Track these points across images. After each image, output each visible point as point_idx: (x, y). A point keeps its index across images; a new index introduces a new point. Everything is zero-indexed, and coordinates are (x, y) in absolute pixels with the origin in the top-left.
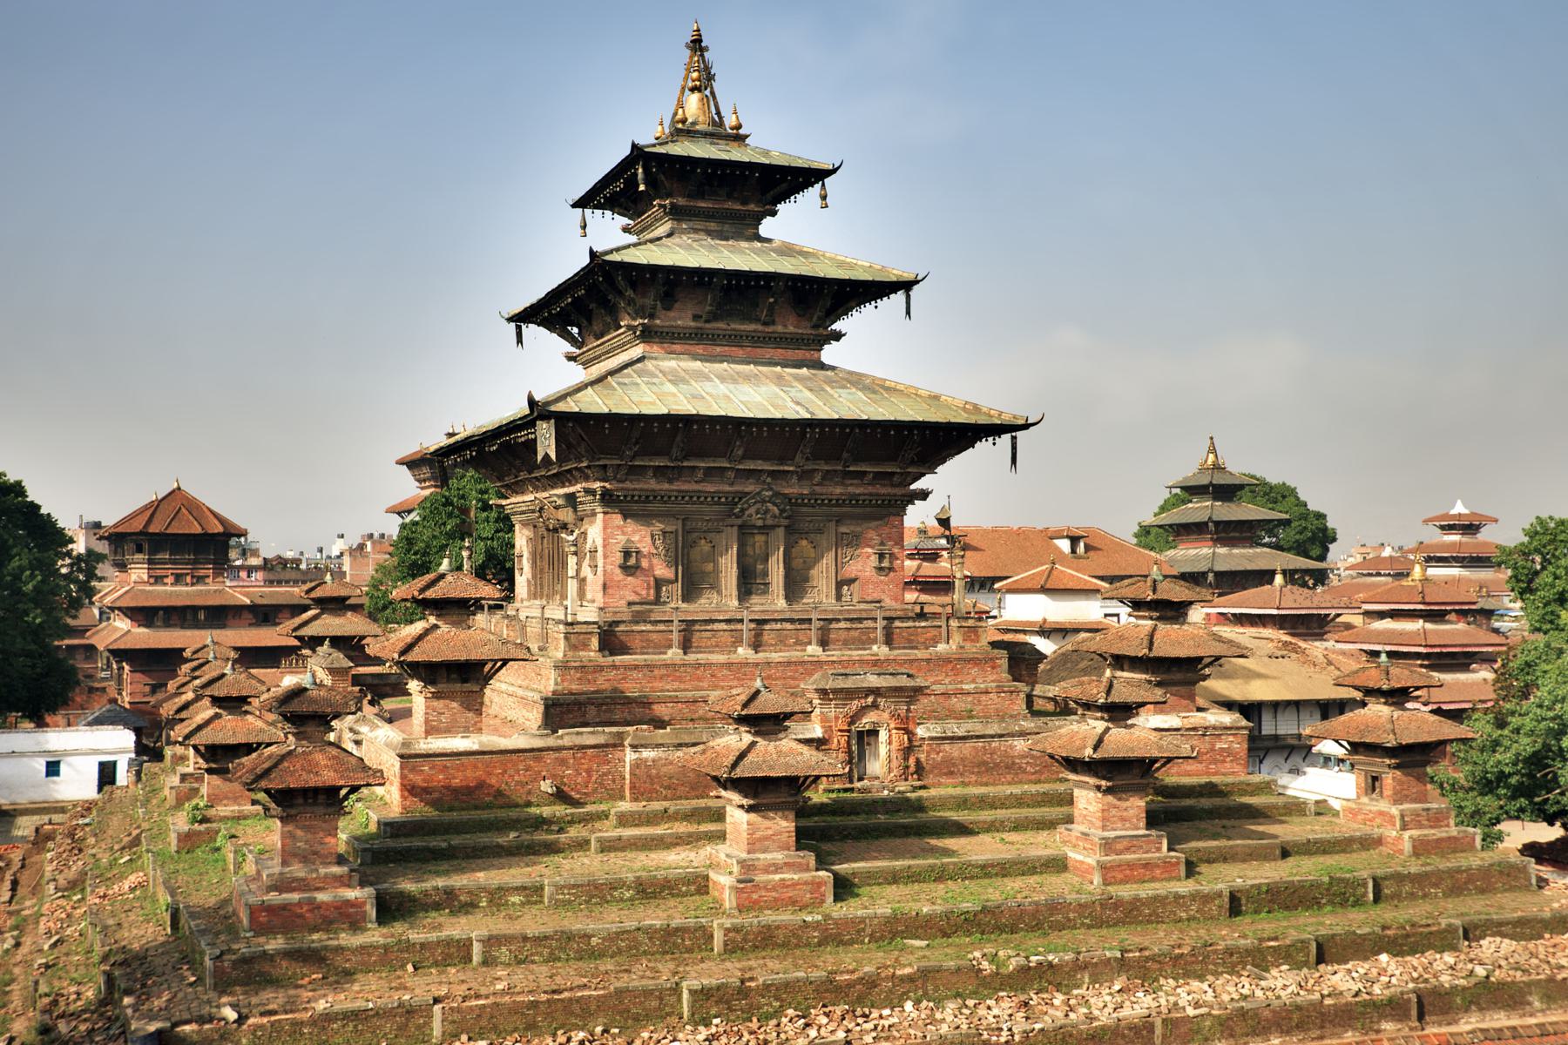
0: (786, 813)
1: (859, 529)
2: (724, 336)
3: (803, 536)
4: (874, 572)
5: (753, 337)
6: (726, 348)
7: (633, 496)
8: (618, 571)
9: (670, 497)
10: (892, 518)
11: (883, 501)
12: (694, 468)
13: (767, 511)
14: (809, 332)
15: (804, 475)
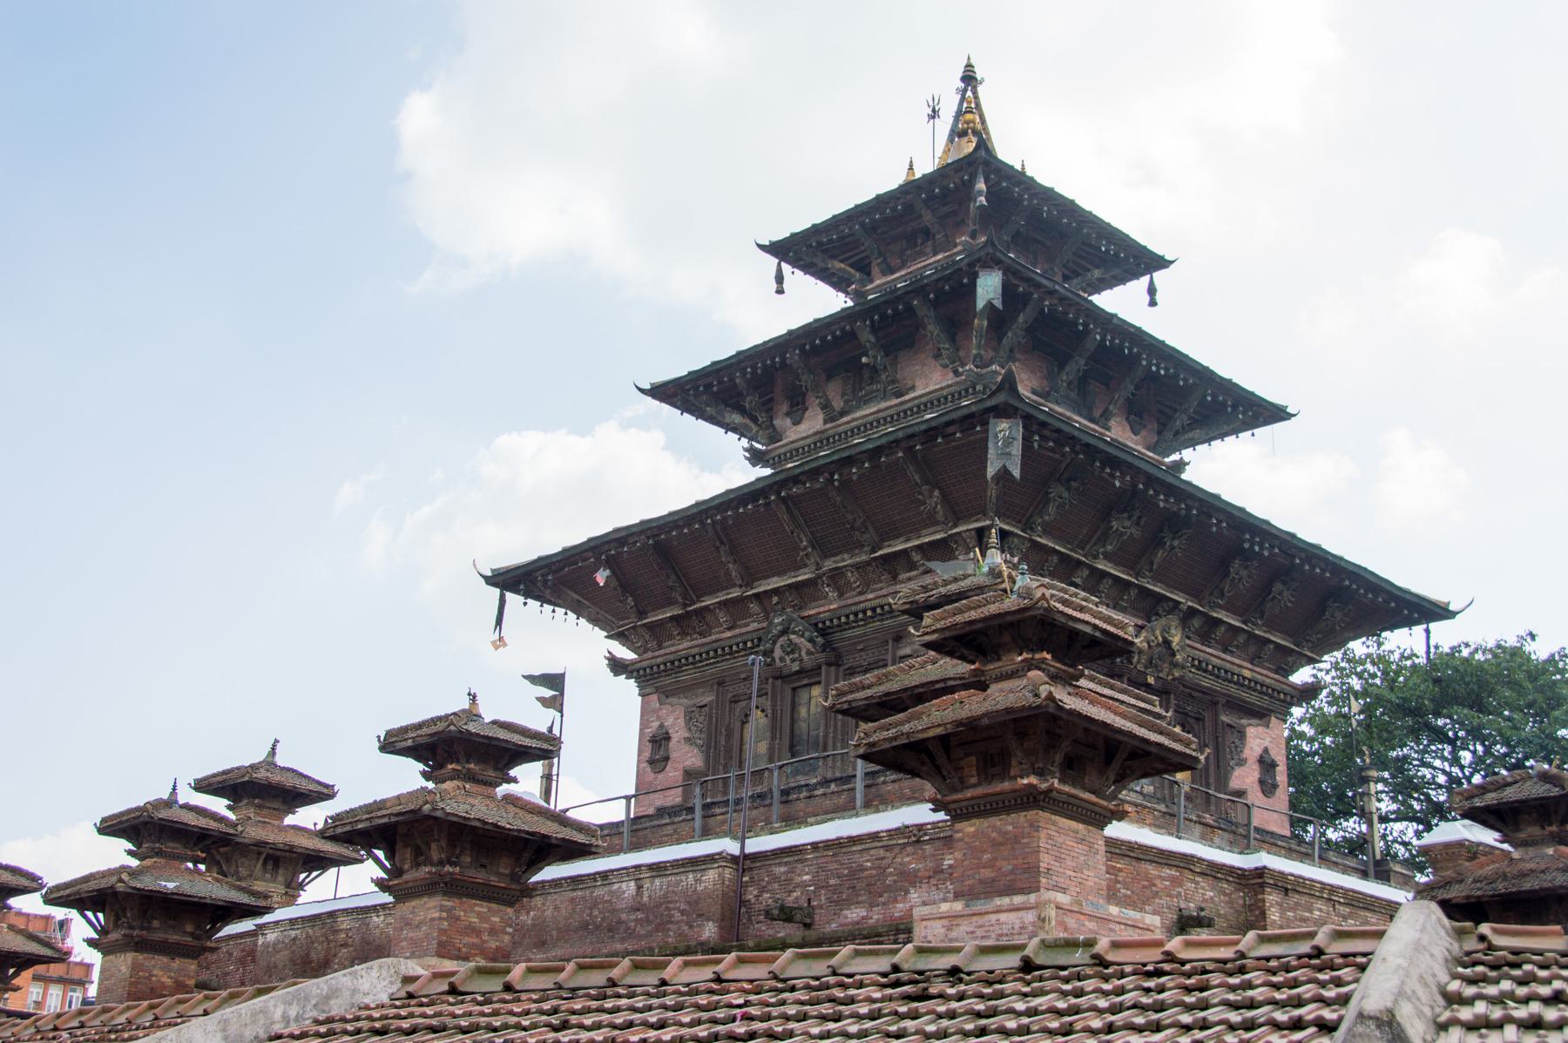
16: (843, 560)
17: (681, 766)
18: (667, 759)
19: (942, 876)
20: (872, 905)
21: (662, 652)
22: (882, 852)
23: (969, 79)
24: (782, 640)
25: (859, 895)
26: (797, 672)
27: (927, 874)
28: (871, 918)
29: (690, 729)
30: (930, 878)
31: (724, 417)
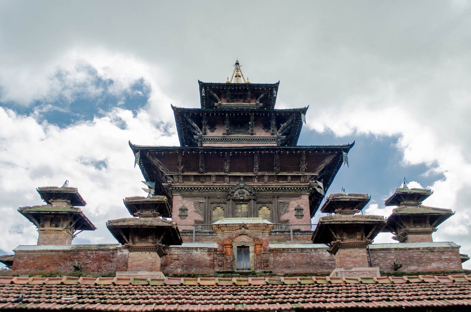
0: (151, 253)
1: (288, 200)
2: (235, 139)
3: (264, 205)
4: (295, 218)
5: (247, 139)
6: (237, 144)
7: (185, 188)
8: (179, 218)
9: (201, 188)
10: (303, 196)
11: (297, 188)
12: (210, 176)
13: (244, 193)
14: (269, 136)
15: (260, 178)
16: (265, 173)
17: (193, 219)
18: (187, 216)
19: (442, 261)
20: (419, 266)
21: (184, 184)
22: (420, 253)
23: (237, 64)
24: (239, 190)
25: (413, 263)
26: (242, 200)
27: (437, 260)
28: (419, 269)
29: (196, 209)
30: (438, 261)
31: (192, 123)
